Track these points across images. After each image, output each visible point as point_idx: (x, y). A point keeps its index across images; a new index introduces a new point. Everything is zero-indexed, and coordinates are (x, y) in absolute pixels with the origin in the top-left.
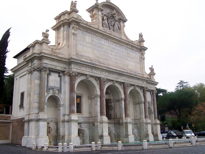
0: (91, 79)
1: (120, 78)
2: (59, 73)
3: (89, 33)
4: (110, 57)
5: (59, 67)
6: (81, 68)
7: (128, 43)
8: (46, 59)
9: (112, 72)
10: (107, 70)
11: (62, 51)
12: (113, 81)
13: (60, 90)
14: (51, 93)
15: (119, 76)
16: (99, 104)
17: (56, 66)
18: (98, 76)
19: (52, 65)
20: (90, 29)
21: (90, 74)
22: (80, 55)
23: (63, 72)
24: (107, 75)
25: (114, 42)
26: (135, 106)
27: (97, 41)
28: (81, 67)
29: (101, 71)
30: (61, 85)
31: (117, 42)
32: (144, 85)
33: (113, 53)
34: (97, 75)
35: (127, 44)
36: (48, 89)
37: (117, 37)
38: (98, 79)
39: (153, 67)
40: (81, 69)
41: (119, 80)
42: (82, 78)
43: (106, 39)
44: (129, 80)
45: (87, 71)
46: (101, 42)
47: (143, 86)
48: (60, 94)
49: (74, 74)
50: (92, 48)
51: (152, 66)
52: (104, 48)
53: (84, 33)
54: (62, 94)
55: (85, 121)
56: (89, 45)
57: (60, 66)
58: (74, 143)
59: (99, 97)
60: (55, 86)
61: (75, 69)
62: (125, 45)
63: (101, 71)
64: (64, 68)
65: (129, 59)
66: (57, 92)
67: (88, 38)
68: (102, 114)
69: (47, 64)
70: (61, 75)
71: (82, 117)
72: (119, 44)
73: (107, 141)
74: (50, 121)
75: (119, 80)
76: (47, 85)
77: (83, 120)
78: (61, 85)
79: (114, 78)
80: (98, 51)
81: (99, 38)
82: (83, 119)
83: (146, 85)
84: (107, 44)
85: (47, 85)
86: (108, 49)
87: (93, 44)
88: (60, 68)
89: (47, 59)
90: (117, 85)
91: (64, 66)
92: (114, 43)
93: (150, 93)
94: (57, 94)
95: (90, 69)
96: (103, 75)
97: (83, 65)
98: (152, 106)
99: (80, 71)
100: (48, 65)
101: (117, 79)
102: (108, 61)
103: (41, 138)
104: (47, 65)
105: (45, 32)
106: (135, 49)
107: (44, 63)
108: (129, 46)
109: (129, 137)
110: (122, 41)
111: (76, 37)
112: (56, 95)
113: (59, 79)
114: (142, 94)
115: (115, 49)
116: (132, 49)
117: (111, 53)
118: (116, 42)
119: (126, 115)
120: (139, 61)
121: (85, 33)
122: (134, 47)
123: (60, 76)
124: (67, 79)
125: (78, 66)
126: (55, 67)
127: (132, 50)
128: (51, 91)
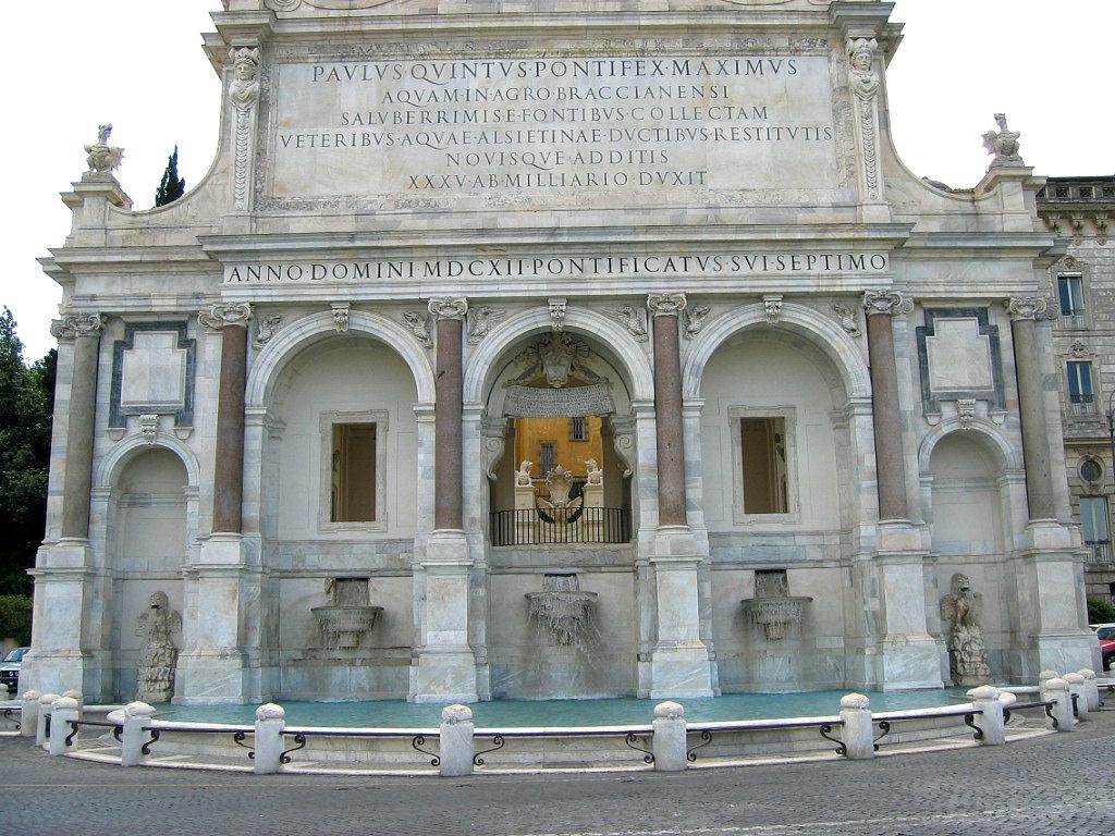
0: (369, 324)
1: (603, 272)
2: (181, 327)
3: (366, 58)
4: (528, 158)
5: (163, 296)
6: (284, 274)
7: (693, 22)
8: (89, 274)
9: (521, 251)
10: (481, 247)
11: (191, 212)
12: (544, 301)
13: (184, 417)
14: (135, 436)
15: (589, 264)
16: (426, 458)
17: (148, 297)
18: (410, 293)
19: (125, 298)
20: (362, 33)
21: (347, 294)
22: (287, 207)
23: (193, 315)
24: (485, 277)
25: (566, 54)
26: (840, 433)
27: (430, 88)
28: (285, 268)
29: (433, 264)
30: (189, 389)
31: (599, 46)
32: (870, 275)
33: (558, 126)
34: (396, 290)
35: (688, 27)
36: (119, 419)
37: (578, 14)
38: (414, 310)
39: (1012, 128)
40: (285, 279)
41: (589, 286)
42: (304, 329)
43: (498, 55)
44: (745, 269)
45: (335, 284)
46: (457, 83)
47: (852, 284)
48: (184, 435)
49: (231, 317)
50: (385, 141)
51: (1001, 119)
52: (480, 115)
53: (328, 68)
54: (197, 432)
55: (392, 565)
56: (359, 130)
57: (164, 296)
58: (203, 689)
59: (433, 418)
60: (152, 398)
61: (237, 290)
62: (679, 44)
63: (433, 264)
64: (197, 296)
65: (710, 128)
66: (169, 423)
67: (357, 89)
68: (449, 512)
69: (93, 298)
70: (192, 334)
71: (377, 542)
72: (613, 53)
73: (449, 680)
74: (174, 575)
75: (595, 289)
76: (115, 401)
77: (378, 558)
78: (189, 389)
79: (545, 287)
80: (433, 141)
81: (439, 64)
82: (383, 551)
83: (881, 276)
84: (510, 84)
85: (115, 401)
86: (517, 113)
87: (389, 120)
88: (174, 302)
89: (97, 274)
90: (591, 323)
91: (201, 285)
92: (569, 62)
93: (983, 321)
94: (166, 437)
95: (351, 268)
96: (448, 287)
97: (292, 258)
98: (999, 420)
99: (274, 292)
100: (100, 303)
101: (573, 286)
102: (513, 181)
103: (45, 660)
104: (95, 303)
105: (94, 141)
106: (783, 43)
107: (84, 297)
108: (707, 43)
109: (655, 657)
110: (640, 27)
111: (253, 114)
112: (162, 442)
113: (178, 358)
114: (852, 355)
115: (582, 93)
116: (755, 52)
117: (542, 127)
118: (587, 44)
119: (675, 512)
120: (825, 118)
121: (339, 67)
122: (761, 30)
123: (186, 343)
124: (211, 350)
125: (264, 271)
126: (144, 302)
127: (755, 61)
128: (135, 427)
